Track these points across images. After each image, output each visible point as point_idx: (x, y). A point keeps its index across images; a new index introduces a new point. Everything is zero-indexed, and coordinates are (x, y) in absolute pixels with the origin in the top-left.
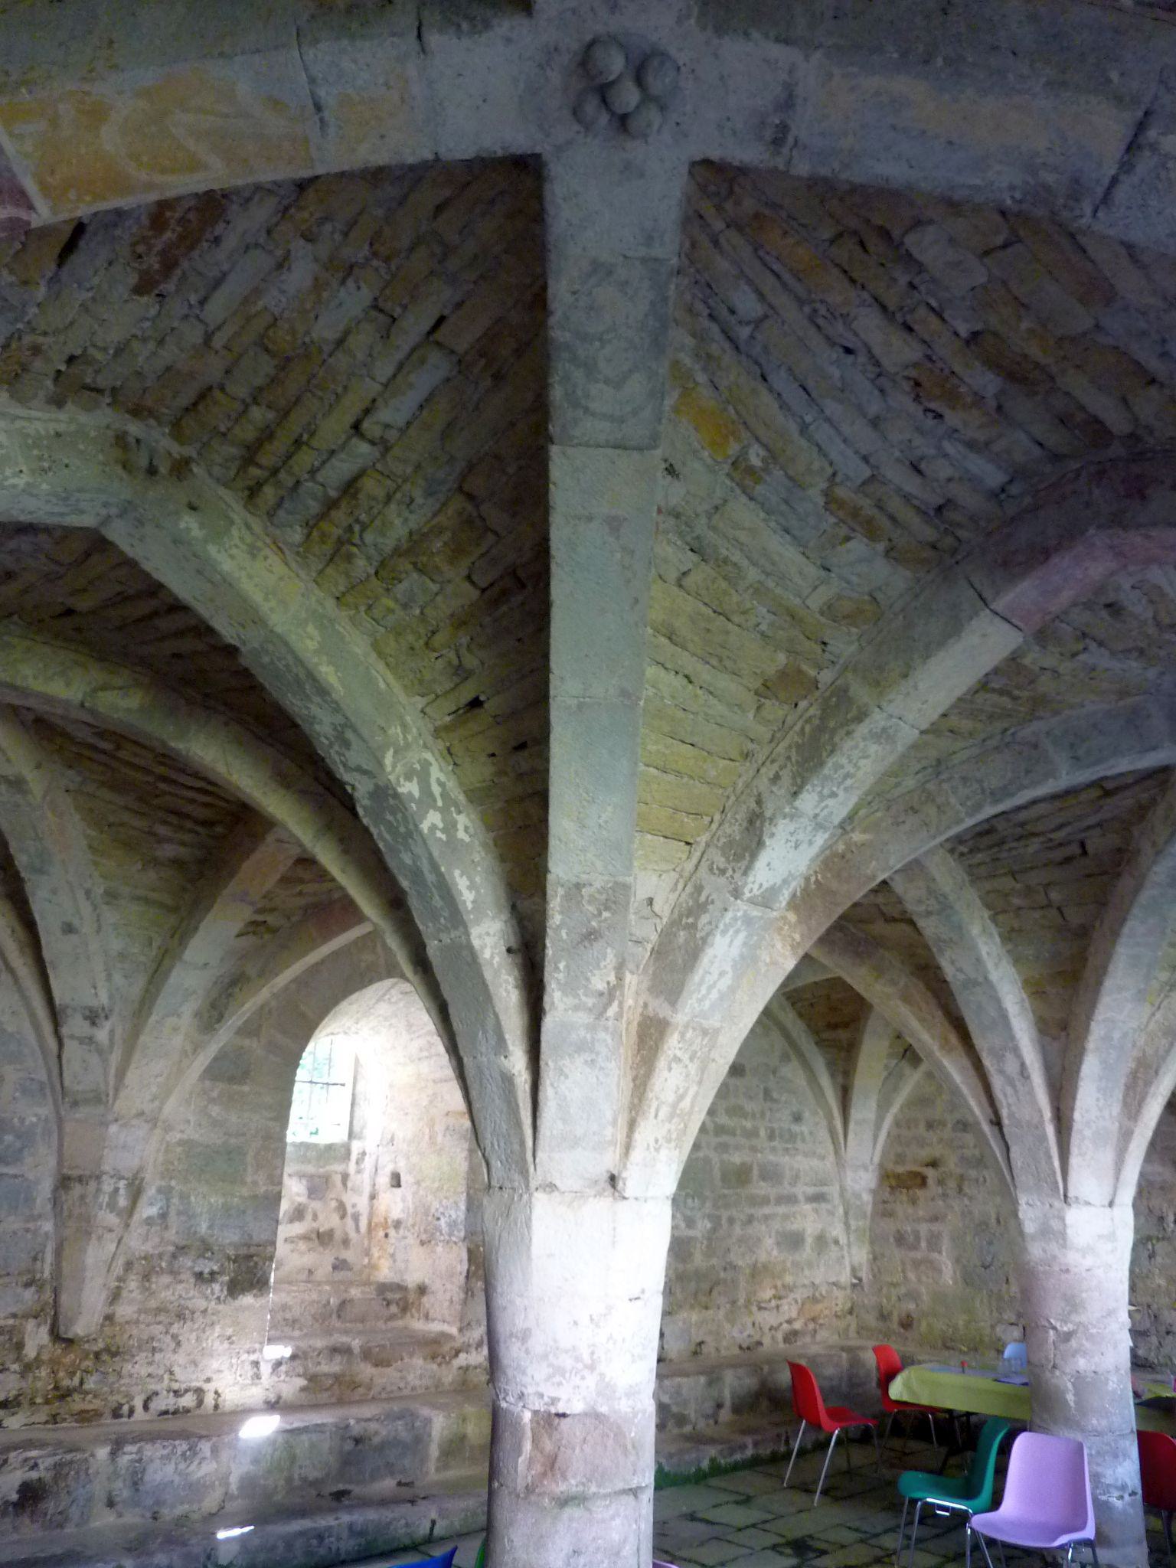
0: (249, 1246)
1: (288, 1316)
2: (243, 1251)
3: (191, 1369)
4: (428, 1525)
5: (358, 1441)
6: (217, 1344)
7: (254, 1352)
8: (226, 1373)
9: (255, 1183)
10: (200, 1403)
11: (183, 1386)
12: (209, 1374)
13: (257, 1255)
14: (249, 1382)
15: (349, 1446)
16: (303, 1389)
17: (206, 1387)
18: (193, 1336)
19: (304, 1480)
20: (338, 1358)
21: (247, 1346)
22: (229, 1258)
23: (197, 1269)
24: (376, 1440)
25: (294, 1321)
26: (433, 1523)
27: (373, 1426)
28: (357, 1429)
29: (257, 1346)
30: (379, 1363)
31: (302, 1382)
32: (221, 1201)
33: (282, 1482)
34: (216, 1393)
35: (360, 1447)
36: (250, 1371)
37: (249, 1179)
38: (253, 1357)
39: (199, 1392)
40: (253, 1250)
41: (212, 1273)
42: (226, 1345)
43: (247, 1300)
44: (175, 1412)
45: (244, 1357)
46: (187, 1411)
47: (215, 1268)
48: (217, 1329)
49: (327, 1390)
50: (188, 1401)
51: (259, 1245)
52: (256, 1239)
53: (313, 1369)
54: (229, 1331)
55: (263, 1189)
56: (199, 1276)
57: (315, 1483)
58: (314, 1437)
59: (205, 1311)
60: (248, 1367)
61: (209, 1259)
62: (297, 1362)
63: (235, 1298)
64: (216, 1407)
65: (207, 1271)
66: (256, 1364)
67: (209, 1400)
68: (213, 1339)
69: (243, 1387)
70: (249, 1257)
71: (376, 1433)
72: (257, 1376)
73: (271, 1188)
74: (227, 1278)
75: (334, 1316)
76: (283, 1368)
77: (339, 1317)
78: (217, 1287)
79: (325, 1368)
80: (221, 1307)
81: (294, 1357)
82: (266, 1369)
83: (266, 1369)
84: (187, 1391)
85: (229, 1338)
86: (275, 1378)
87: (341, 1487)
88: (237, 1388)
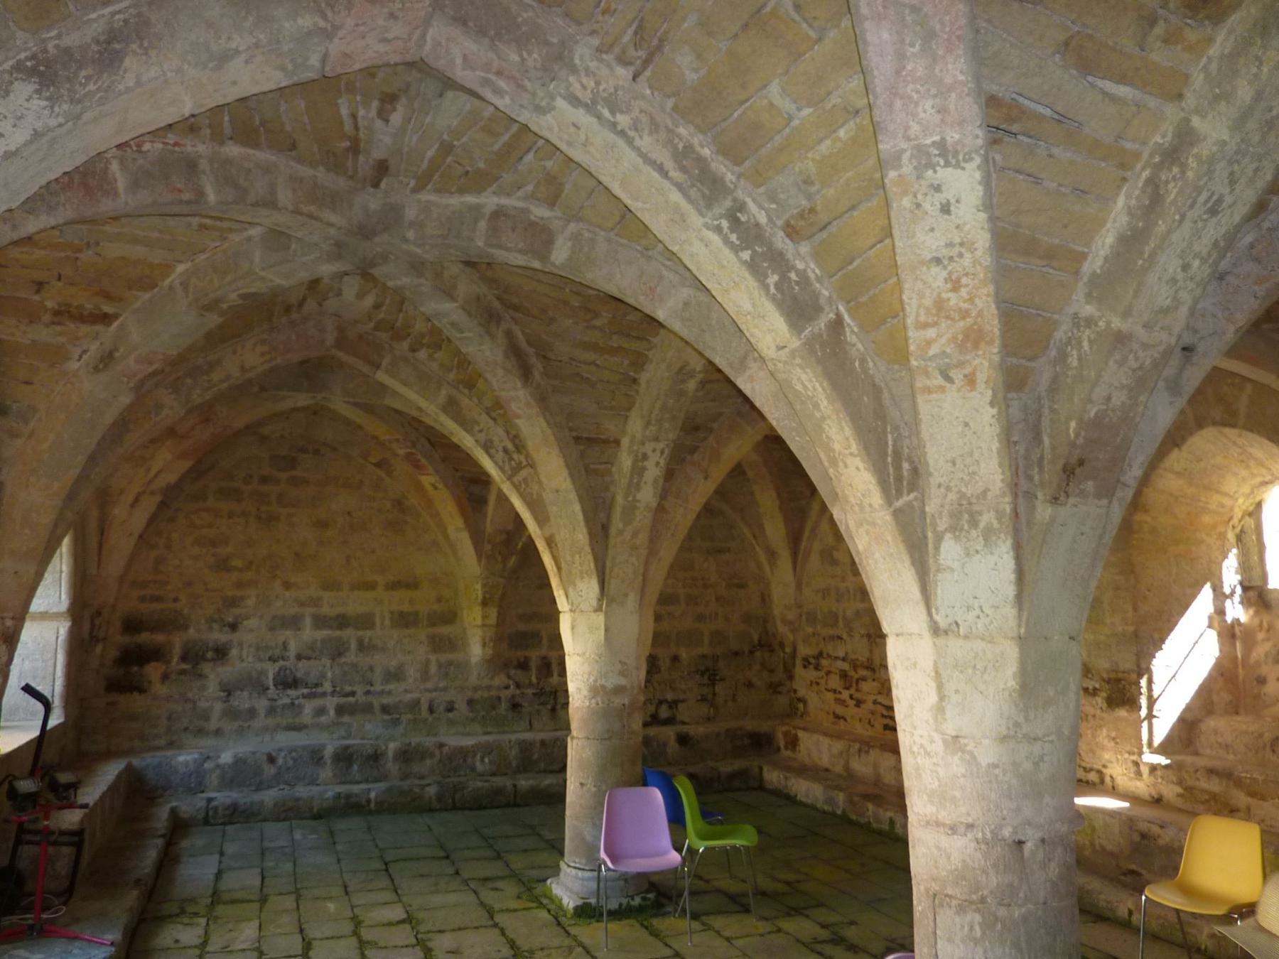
0: (1117, 672)
1: (1220, 740)
2: (1113, 676)
3: (1091, 755)
4: (1126, 911)
5: (1144, 836)
6: (1106, 742)
7: (1134, 754)
8: (1115, 764)
9: (1113, 624)
10: (1102, 781)
11: (1088, 766)
12: (1103, 762)
13: (1124, 680)
14: (1132, 775)
15: (1137, 838)
16: (1179, 795)
17: (1104, 770)
18: (1089, 732)
19: (1103, 848)
20: (1215, 780)
21: (1128, 748)
22: (1104, 680)
23: (1084, 685)
24: (1161, 842)
25: (1227, 747)
26: (1130, 913)
27: (1155, 830)
28: (1143, 826)
29: (1136, 750)
30: (1252, 794)
31: (1179, 790)
32: (1092, 637)
33: (1087, 843)
34: (1111, 777)
35: (1146, 842)
36: (1133, 769)
37: (1108, 621)
38: (1134, 758)
39: (1099, 772)
40: (1120, 675)
41: (1095, 689)
42: (1112, 744)
43: (1122, 713)
44: (1087, 782)
45: (1126, 756)
46: (1094, 784)
47: (1097, 686)
48: (1105, 732)
49: (1202, 803)
50: (1093, 777)
51: (1124, 672)
52: (1121, 668)
53: (1190, 782)
54: (1113, 734)
55: (1120, 629)
56: (1086, 690)
57: (1111, 854)
58: (1107, 818)
59: (1094, 716)
60: (1130, 765)
61: (1091, 679)
62: (1170, 772)
63: (1113, 710)
64: (1113, 788)
65: (1091, 687)
66: (1136, 764)
67: (1108, 780)
68: (1103, 736)
69: (1131, 779)
70: (1119, 680)
71: (1159, 836)
72: (1139, 774)
73: (1126, 628)
74: (1104, 694)
75: (1268, 749)
76: (1159, 773)
77: (1273, 751)
78: (1099, 700)
79: (1204, 784)
80: (1104, 715)
81: (1167, 767)
82: (1145, 771)
83: (1145, 771)
84: (1091, 770)
85: (1114, 739)
86: (1152, 778)
87: (1134, 867)
88: (1125, 778)
